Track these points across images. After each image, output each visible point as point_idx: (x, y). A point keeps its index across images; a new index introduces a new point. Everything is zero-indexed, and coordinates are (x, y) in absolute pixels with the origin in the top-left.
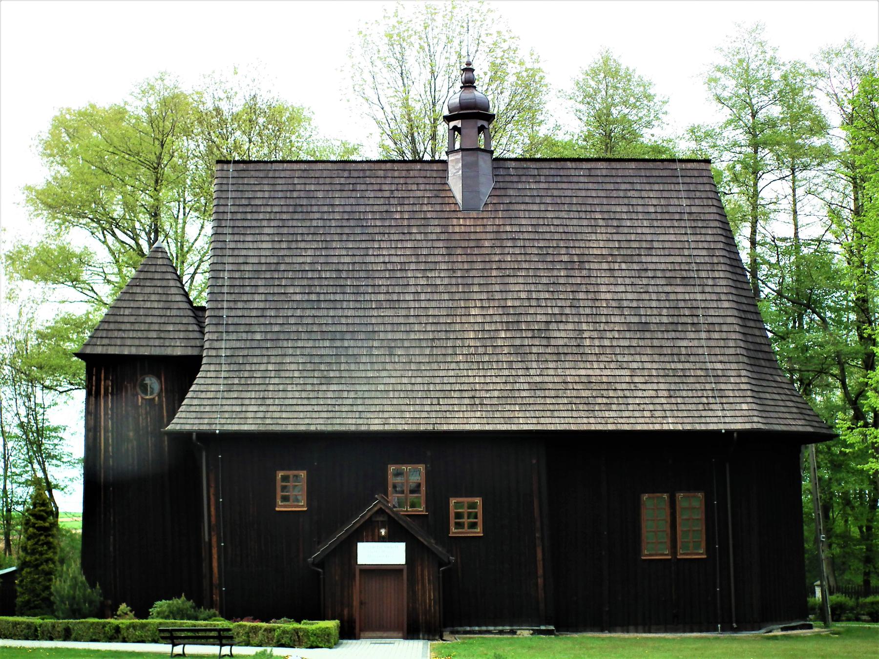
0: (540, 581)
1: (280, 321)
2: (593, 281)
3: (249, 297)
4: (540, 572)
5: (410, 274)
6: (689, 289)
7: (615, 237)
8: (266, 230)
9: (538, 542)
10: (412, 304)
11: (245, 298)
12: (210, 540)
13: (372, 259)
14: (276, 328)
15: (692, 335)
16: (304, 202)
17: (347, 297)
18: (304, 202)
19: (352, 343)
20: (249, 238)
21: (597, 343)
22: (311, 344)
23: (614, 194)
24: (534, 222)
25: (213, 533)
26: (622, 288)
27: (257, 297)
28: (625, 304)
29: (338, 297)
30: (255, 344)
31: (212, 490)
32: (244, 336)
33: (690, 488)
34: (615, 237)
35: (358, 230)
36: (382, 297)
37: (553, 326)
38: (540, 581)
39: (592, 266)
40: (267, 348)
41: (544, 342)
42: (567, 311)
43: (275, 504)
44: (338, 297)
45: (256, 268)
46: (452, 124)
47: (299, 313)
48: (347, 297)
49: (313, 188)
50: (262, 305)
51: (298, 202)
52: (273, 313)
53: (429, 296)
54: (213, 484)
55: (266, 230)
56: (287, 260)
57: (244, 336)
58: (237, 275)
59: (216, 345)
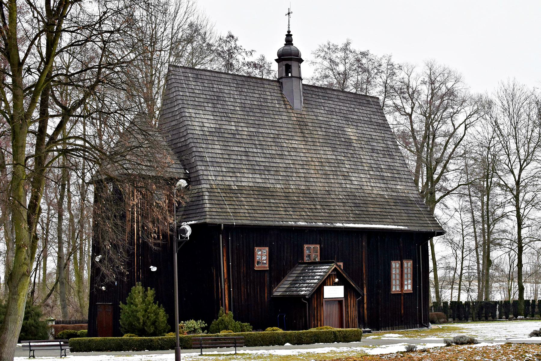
0: (365, 306)
1: (232, 161)
2: (357, 152)
3: (213, 146)
4: (365, 301)
5: (283, 141)
6: (391, 160)
7: (358, 131)
8: (207, 108)
9: (365, 286)
10: (289, 157)
11: (210, 146)
12: (224, 287)
13: (263, 131)
14: (232, 166)
15: (399, 183)
16: (221, 95)
17: (259, 151)
18: (221, 95)
19: (270, 177)
20: (201, 112)
21: (369, 184)
22: (250, 176)
23: (350, 109)
24: (325, 119)
25: (225, 283)
26: (368, 157)
27: (216, 147)
28: (373, 165)
29: (255, 150)
30: (225, 174)
31: (225, 258)
32: (218, 169)
33: (408, 258)
34: (358, 131)
35: (251, 114)
36: (274, 152)
37: (350, 174)
38: (365, 306)
39: (355, 145)
40: (231, 177)
41: (349, 182)
42: (353, 167)
43: (254, 266)
44: (255, 150)
45: (210, 130)
46: (285, 63)
47: (239, 157)
48: (259, 151)
49: (222, 87)
50: (220, 152)
51: (217, 94)
52: (227, 156)
53: (295, 154)
54: (225, 255)
55: (207, 108)
56: (224, 127)
57: (218, 169)
58: (201, 133)
59: (205, 173)
